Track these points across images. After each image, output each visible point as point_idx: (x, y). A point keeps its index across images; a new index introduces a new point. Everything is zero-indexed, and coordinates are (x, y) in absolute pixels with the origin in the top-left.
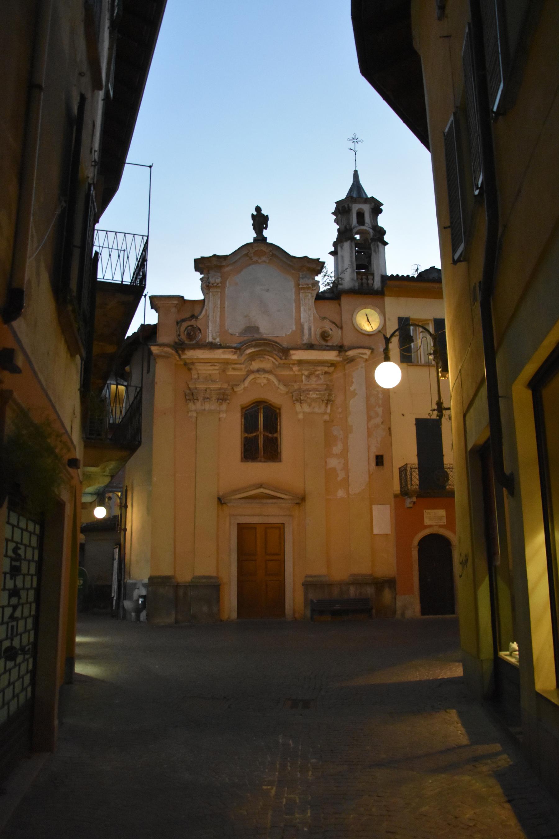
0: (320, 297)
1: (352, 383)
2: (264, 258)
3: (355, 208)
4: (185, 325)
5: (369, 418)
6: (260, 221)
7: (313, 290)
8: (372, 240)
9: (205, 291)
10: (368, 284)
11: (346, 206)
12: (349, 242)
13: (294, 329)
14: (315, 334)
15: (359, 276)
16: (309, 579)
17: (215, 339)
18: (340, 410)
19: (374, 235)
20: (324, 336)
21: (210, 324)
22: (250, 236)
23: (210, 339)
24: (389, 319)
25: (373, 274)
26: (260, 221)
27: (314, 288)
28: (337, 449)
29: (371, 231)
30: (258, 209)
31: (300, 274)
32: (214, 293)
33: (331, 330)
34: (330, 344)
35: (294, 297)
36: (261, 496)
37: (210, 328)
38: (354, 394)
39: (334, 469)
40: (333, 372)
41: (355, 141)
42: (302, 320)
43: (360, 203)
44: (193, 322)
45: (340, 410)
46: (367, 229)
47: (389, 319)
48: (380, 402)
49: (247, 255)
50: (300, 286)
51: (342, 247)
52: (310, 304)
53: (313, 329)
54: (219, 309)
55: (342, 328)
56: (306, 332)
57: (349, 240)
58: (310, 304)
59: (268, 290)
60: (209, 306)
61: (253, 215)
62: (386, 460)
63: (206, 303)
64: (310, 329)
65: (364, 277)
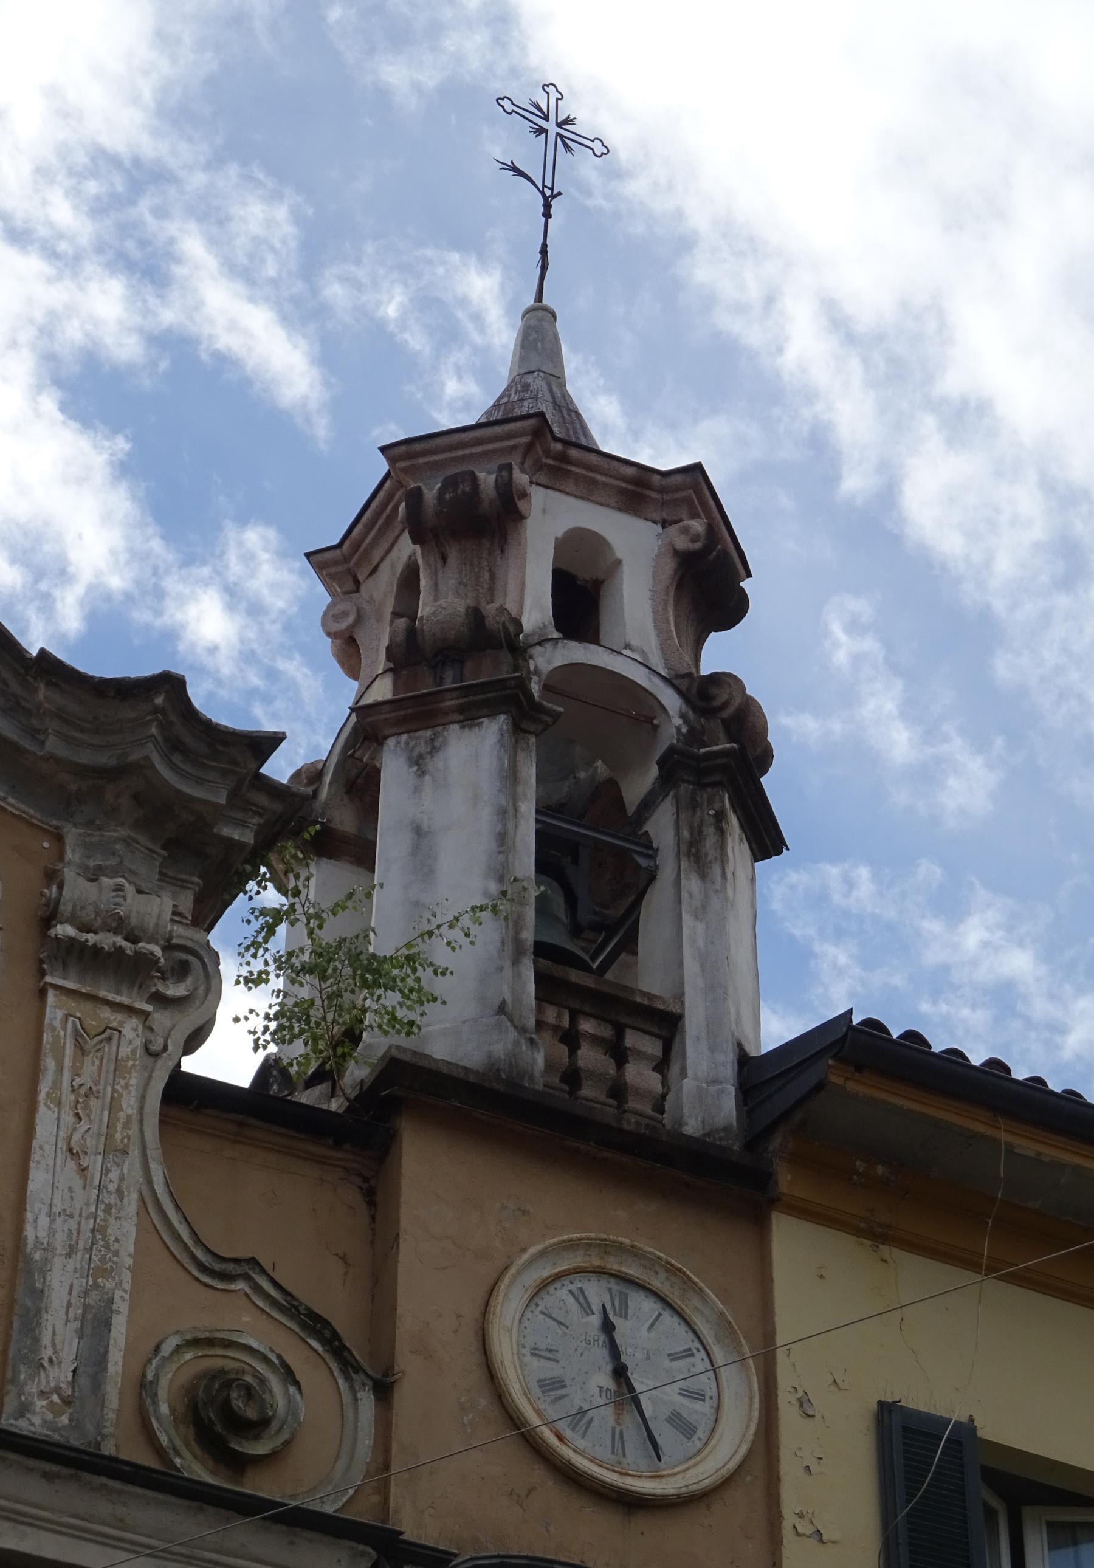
0: (192, 1097)
3: (551, 517)
7: (161, 1000)
10: (618, 1091)
11: (487, 479)
12: (492, 731)
15: (551, 1015)
19: (694, 736)
20: (225, 1417)
25: (667, 1024)
27: (174, 990)
29: (670, 700)
31: (72, 834)
33: (289, 1376)
34: (259, 1485)
41: (551, 127)
46: (639, 675)
50: (65, 930)
51: (419, 763)
52: (129, 1105)
53: (119, 1327)
58: (129, 1105)
64: (96, 1324)
65: (587, 1026)
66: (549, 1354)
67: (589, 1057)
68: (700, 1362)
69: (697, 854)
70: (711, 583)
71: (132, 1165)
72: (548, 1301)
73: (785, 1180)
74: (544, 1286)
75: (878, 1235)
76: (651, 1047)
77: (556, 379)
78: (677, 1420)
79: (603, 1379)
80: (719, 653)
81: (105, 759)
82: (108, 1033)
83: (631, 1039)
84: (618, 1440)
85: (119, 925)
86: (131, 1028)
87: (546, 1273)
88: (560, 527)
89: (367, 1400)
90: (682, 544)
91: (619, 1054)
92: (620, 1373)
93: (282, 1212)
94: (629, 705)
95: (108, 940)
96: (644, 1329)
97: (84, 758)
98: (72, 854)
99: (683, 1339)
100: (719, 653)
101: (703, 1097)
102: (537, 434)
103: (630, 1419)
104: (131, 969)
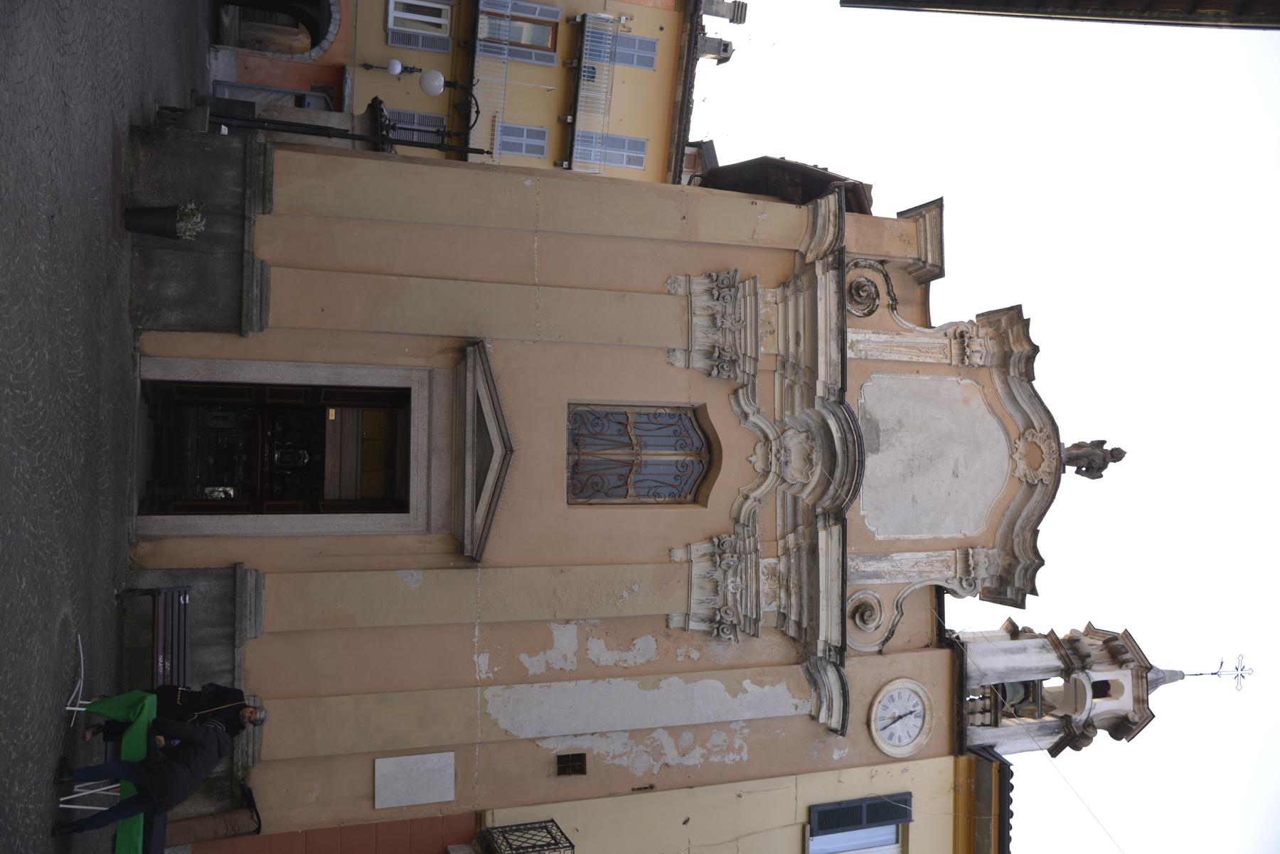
1: (761, 684)
2: (1022, 466)
3: (1123, 677)
4: (879, 280)
5: (675, 731)
6: (1094, 459)
7: (961, 580)
8: (1066, 720)
9: (950, 331)
10: (973, 713)
12: (1059, 663)
13: (879, 537)
14: (865, 588)
15: (988, 691)
16: (251, 580)
17: (851, 347)
18: (695, 655)
20: (862, 612)
21: (884, 337)
22: (1067, 440)
23: (851, 336)
24: (905, 770)
25: (995, 724)
26: (1094, 459)
27: (964, 584)
28: (598, 650)
30: (1117, 455)
31: (995, 551)
32: (947, 350)
34: (849, 622)
35: (945, 536)
36: (481, 449)
37: (874, 337)
38: (736, 690)
39: (548, 644)
40: (784, 634)
42: (896, 556)
43: (1135, 687)
44: (884, 299)
45: (695, 655)
46: (1088, 706)
47: (905, 770)
48: (714, 759)
49: (1030, 425)
51: (1043, 647)
52: (932, 576)
53: (877, 582)
54: (915, 359)
55: (880, 652)
56: (872, 567)
57: (1065, 662)
58: (932, 576)
59: (955, 475)
60: (920, 337)
61: (1104, 442)
62: (572, 782)
63: (927, 330)
64: (877, 575)
65: (988, 702)
66: (900, 697)
67: (980, 703)
68: (909, 740)
69: (1045, 730)
70: (1123, 728)
71: (917, 579)
72: (913, 695)
73: (963, 759)
74: (917, 693)
75: (956, 789)
76: (987, 721)
77: (1164, 682)
78: (891, 736)
79: (897, 715)
80: (1102, 736)
81: (1017, 553)
82: (948, 567)
83: (988, 714)
84: (883, 719)
85: (976, 564)
86: (951, 573)
87: (921, 693)
88: (1122, 680)
89: (877, 649)
90: (1130, 716)
91: (983, 711)
92: (900, 717)
93: (917, 623)
94: (1079, 702)
95: (971, 562)
96: (912, 723)
97: (1016, 549)
98: (990, 552)
99: (914, 734)
100: (1102, 736)
101: (980, 735)
102: (1147, 677)
103: (889, 721)
104: (967, 571)
